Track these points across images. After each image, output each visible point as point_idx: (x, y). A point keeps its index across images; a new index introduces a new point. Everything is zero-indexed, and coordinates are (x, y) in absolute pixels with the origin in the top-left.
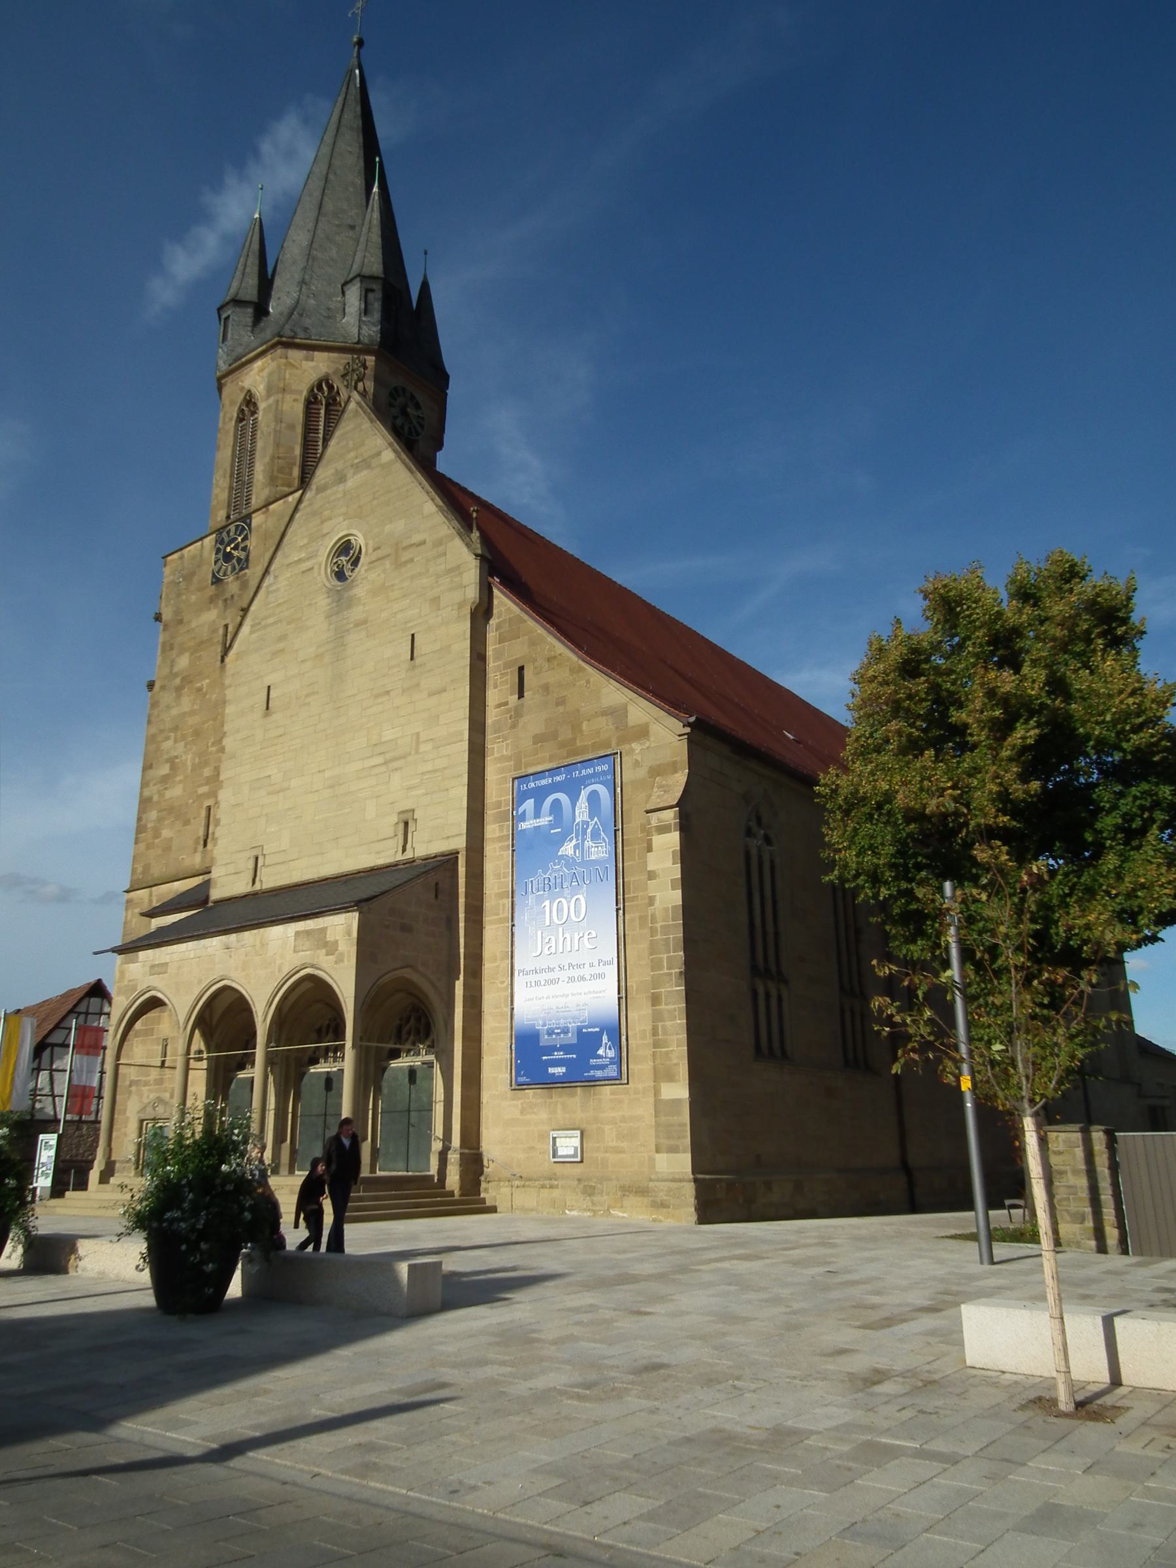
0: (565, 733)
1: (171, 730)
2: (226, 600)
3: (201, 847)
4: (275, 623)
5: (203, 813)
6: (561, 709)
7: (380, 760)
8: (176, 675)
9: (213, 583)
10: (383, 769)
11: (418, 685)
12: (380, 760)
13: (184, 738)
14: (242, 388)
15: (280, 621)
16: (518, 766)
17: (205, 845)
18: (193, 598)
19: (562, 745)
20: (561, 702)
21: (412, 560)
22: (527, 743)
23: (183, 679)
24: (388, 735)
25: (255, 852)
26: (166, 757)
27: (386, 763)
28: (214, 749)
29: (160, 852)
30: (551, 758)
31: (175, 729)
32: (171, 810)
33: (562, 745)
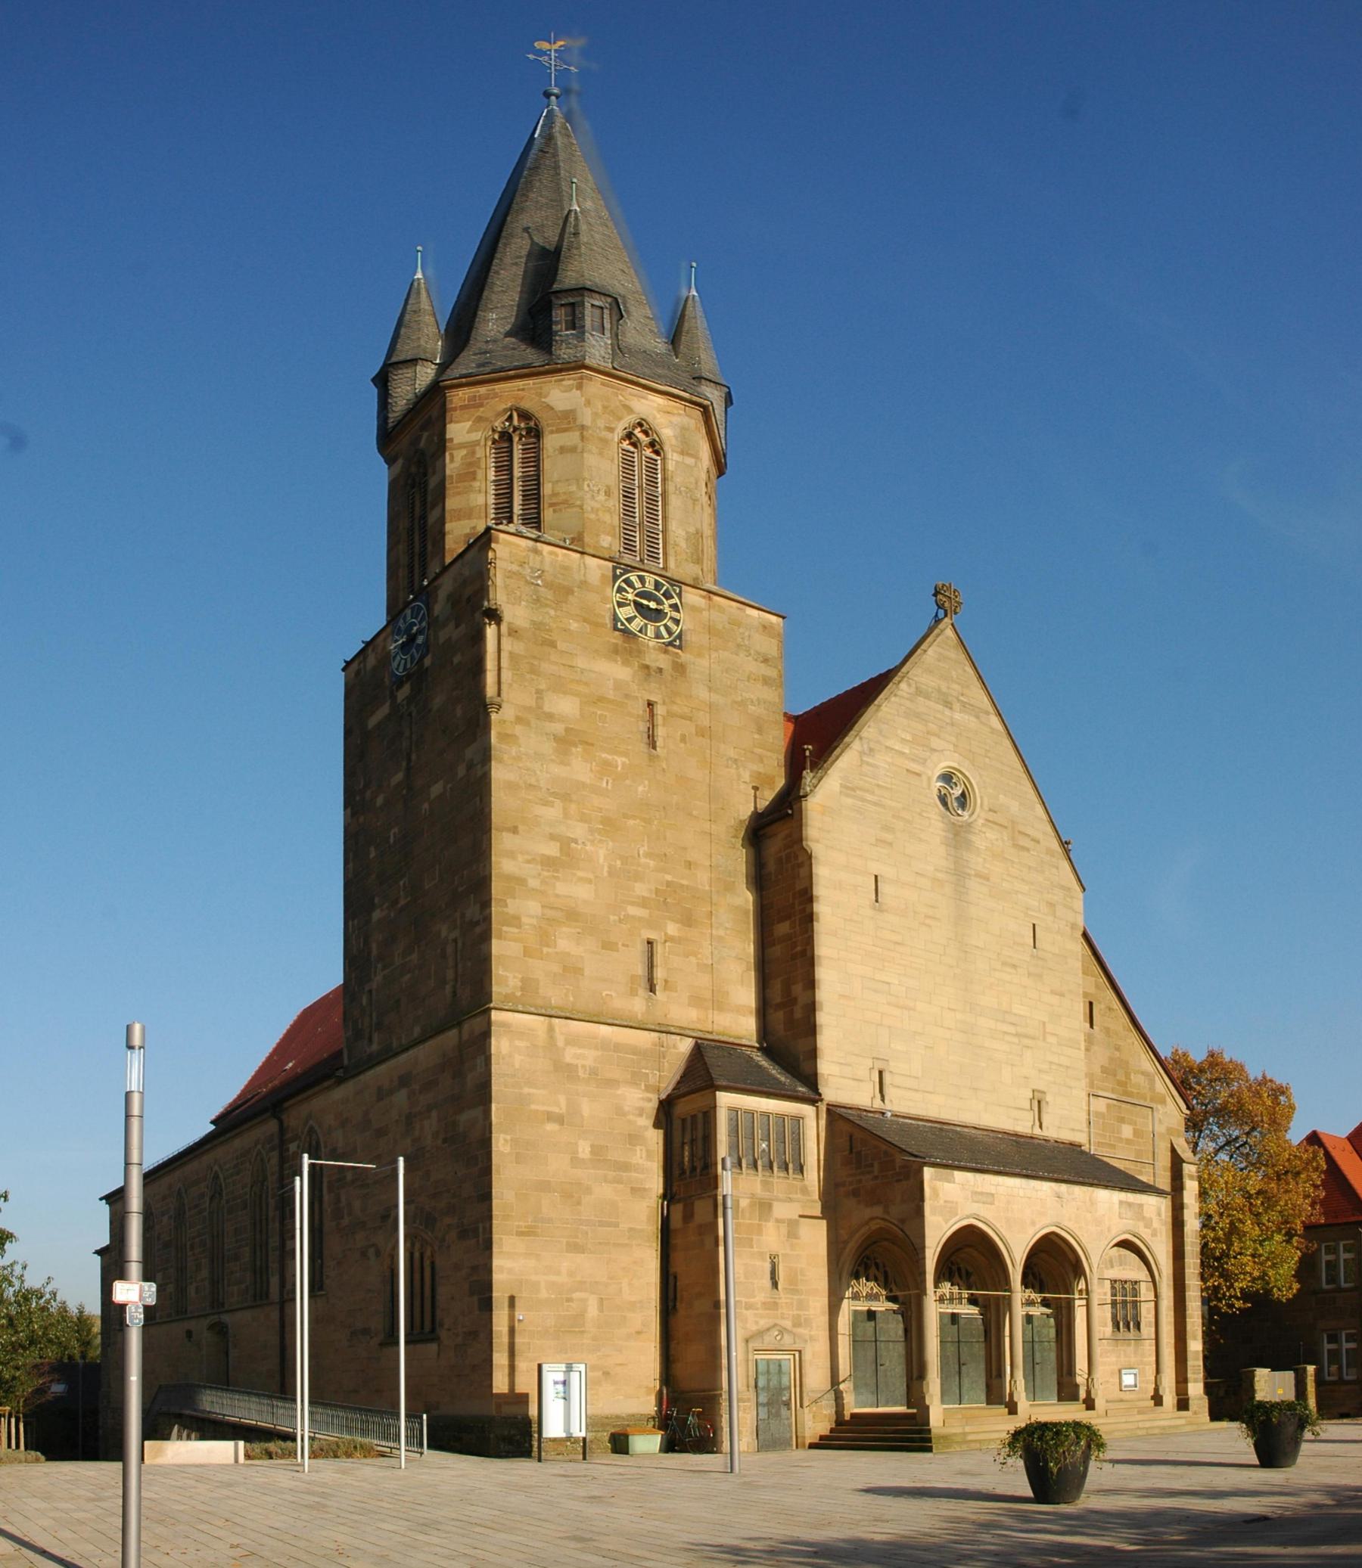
0: (1121, 1077)
1: (554, 794)
5: (640, 948)
6: (1117, 1054)
7: (1012, 1029)
8: (550, 717)
9: (616, 629)
10: (1016, 1040)
13: (584, 818)
16: (1091, 1085)
18: (574, 626)
19: (1120, 1083)
20: (1118, 1049)
22: (1097, 1070)
23: (567, 730)
25: (879, 1065)
27: (1017, 1035)
29: (556, 968)
30: (1113, 1092)
31: (566, 798)
32: (572, 915)
33: (1120, 1083)
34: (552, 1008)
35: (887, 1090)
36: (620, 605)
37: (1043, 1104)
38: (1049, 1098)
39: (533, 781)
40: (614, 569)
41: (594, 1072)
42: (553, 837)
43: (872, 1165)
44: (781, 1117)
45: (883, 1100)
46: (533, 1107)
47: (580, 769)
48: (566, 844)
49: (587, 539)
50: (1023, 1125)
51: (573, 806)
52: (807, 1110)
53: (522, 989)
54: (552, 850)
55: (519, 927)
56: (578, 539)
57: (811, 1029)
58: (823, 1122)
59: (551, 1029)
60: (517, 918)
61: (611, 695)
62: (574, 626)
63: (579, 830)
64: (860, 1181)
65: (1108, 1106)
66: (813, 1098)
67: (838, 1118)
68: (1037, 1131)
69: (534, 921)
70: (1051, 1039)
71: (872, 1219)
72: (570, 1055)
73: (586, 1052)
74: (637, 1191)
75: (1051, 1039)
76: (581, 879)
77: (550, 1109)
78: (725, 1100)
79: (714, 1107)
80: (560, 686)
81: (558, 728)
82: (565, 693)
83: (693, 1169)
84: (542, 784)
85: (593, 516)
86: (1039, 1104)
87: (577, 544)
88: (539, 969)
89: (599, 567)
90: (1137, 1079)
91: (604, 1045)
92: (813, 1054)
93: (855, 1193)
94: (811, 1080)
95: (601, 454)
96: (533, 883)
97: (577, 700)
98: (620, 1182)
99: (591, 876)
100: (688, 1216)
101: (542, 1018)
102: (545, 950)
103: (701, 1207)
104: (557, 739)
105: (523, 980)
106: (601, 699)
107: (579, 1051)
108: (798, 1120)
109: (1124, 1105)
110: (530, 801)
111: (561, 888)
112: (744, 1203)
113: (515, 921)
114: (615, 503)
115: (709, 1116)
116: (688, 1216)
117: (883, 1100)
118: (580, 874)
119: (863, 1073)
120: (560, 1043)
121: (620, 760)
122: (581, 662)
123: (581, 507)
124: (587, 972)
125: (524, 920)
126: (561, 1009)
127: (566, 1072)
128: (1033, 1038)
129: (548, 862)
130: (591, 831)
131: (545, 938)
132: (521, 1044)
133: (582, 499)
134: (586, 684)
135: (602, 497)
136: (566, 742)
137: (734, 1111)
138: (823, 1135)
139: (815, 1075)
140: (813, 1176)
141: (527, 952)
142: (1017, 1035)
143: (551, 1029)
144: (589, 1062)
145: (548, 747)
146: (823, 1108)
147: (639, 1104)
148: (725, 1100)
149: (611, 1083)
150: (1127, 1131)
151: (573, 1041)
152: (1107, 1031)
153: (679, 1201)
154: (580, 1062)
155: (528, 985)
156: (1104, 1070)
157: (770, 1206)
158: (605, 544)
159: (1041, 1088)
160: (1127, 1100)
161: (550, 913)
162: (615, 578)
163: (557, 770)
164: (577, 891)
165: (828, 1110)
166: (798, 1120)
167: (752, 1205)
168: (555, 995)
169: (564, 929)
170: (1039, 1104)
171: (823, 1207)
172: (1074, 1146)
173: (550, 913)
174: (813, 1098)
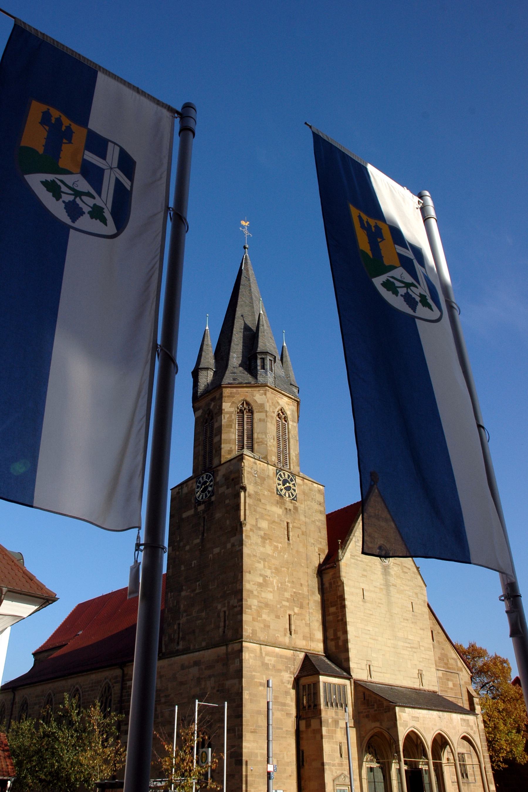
0: (445, 661)
1: (261, 559)
2: (286, 509)
3: (288, 635)
4: (361, 561)
7: (409, 645)
8: (260, 529)
9: (277, 494)
10: (410, 649)
11: (416, 623)
12: (409, 645)
13: (270, 568)
14: (278, 402)
15: (363, 562)
16: (436, 666)
17: (291, 634)
18: (266, 493)
20: (443, 649)
21: (407, 573)
23: (264, 534)
24: (410, 637)
25: (369, 663)
26: (259, 572)
27: (411, 647)
28: (289, 585)
29: (262, 626)
30: (444, 667)
31: (264, 560)
32: (267, 605)
34: (261, 641)
35: (372, 673)
36: (279, 484)
37: (422, 675)
38: (424, 673)
39: (255, 553)
40: (277, 470)
41: (274, 666)
42: (261, 575)
43: (374, 705)
44: (339, 685)
45: (371, 677)
46: (256, 680)
47: (268, 549)
48: (265, 577)
49: (268, 458)
50: (415, 684)
51: (266, 563)
52: (347, 682)
53: (252, 634)
54: (261, 580)
55: (251, 609)
56: (266, 458)
57: (346, 650)
58: (353, 687)
59: (261, 649)
60: (251, 606)
61: (277, 520)
62: (266, 493)
63: (268, 573)
64: (369, 711)
65: (443, 674)
66: (349, 677)
67: (358, 685)
68: (421, 687)
69: (255, 607)
70: (422, 648)
71: (375, 728)
72: (267, 659)
73: (271, 658)
74: (288, 715)
75: (422, 648)
76: (269, 591)
77: (261, 681)
78: (323, 679)
79: (319, 682)
80: (262, 517)
81: (262, 533)
82: (264, 520)
83: (309, 706)
84: (258, 555)
85: (270, 449)
86: (421, 675)
87: (265, 459)
88: (258, 626)
89: (272, 469)
90: (451, 661)
91: (277, 656)
92: (348, 660)
93: (367, 716)
94: (347, 670)
95: (271, 423)
96: (255, 593)
97: (267, 522)
98: (283, 711)
99: (271, 590)
100: (308, 725)
101: (258, 645)
102: (259, 618)
103: (314, 723)
104: (262, 538)
105: (253, 630)
106: (274, 522)
107: (269, 658)
108: (344, 686)
109: (448, 673)
110: (254, 561)
111: (263, 595)
112: (330, 721)
113: (250, 607)
114: (275, 443)
115: (316, 684)
116: (308, 725)
117: (371, 677)
118: (269, 589)
119: (364, 667)
120: (264, 655)
121: (280, 545)
122: (268, 507)
123: (266, 445)
124: (271, 627)
125: (253, 607)
126: (264, 641)
127: (265, 666)
128: (416, 648)
129: (260, 585)
130: (272, 573)
131: (259, 615)
132: (252, 655)
133: (267, 441)
134: (269, 516)
135: (272, 441)
136: (265, 538)
137: (325, 683)
138: (353, 692)
139: (349, 668)
140: (350, 709)
141: (254, 620)
142: (411, 647)
143: (261, 649)
144: (272, 662)
145: (259, 540)
146: (352, 681)
147: (288, 678)
148: (323, 679)
149: (279, 671)
150: (450, 684)
151: (267, 654)
152: (438, 642)
153: (304, 719)
154: (269, 662)
155: (254, 632)
156: (440, 659)
157: (338, 722)
158: (273, 460)
159: (421, 669)
160: (449, 671)
161: (260, 604)
162: (277, 474)
163: (262, 549)
164: (269, 596)
165: (354, 682)
166: (344, 686)
167: (332, 721)
168: (262, 636)
169: (264, 610)
170: (421, 675)
171: (354, 722)
172: (435, 692)
173: (260, 604)
174: (349, 677)
